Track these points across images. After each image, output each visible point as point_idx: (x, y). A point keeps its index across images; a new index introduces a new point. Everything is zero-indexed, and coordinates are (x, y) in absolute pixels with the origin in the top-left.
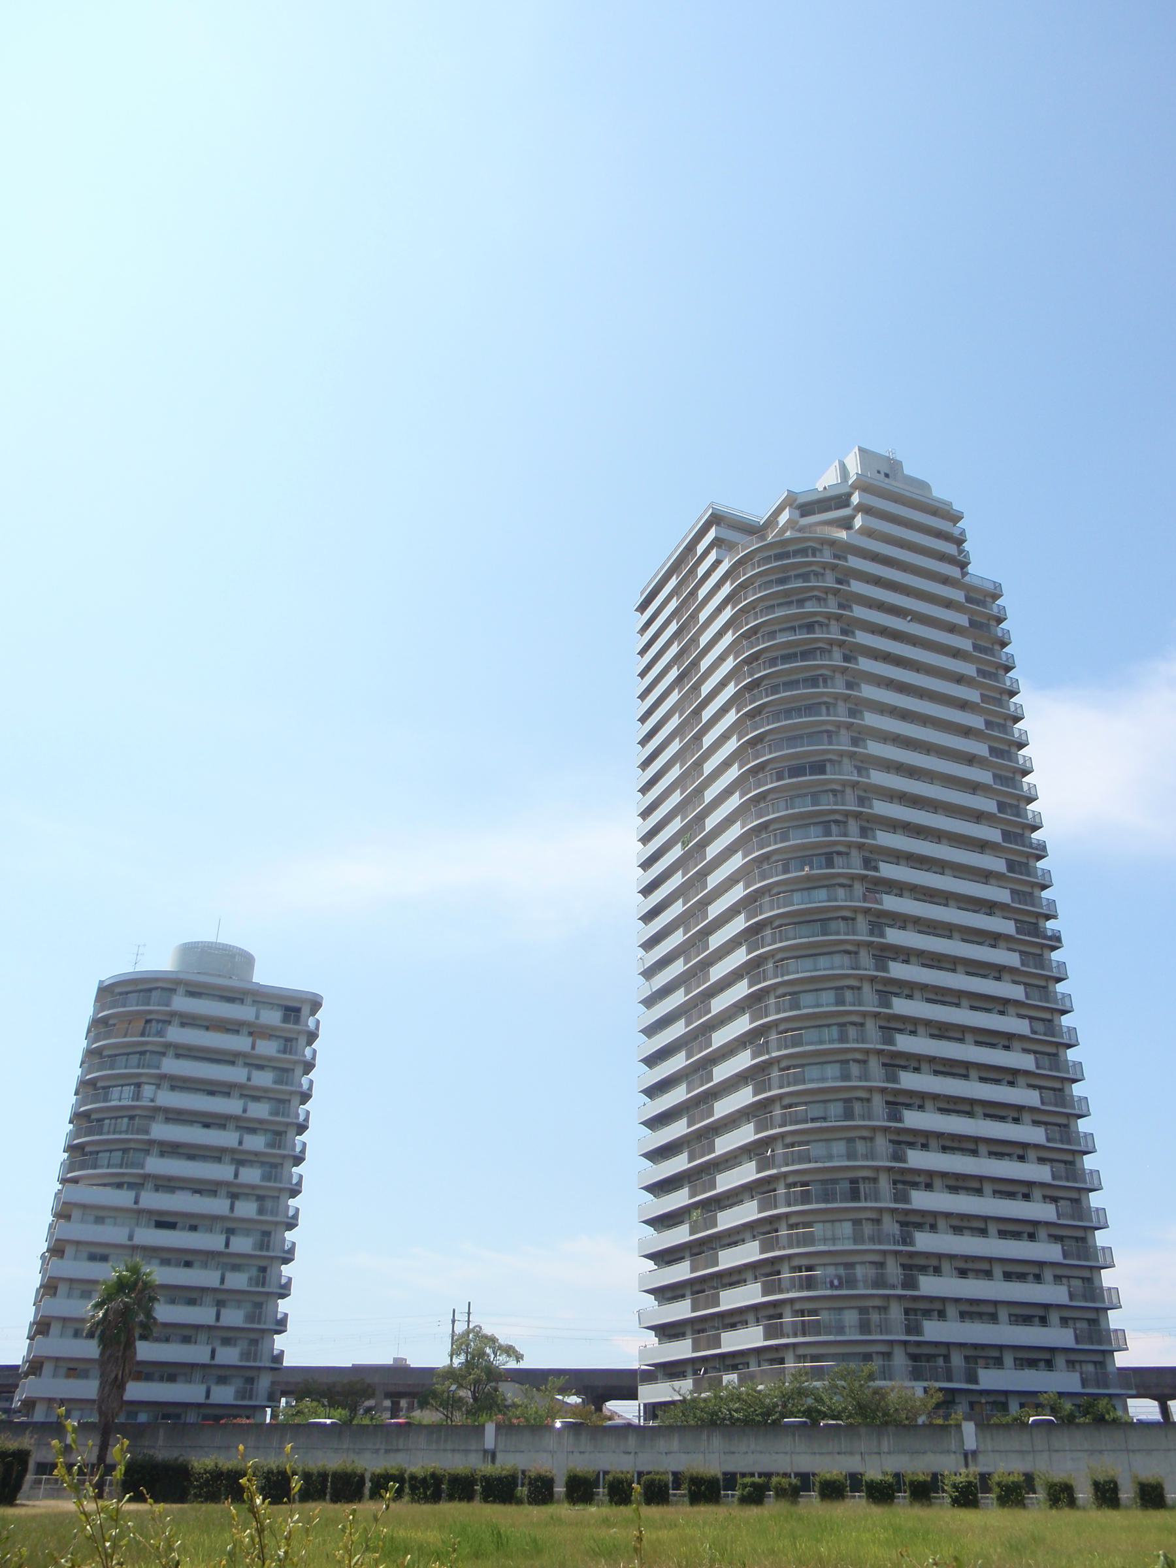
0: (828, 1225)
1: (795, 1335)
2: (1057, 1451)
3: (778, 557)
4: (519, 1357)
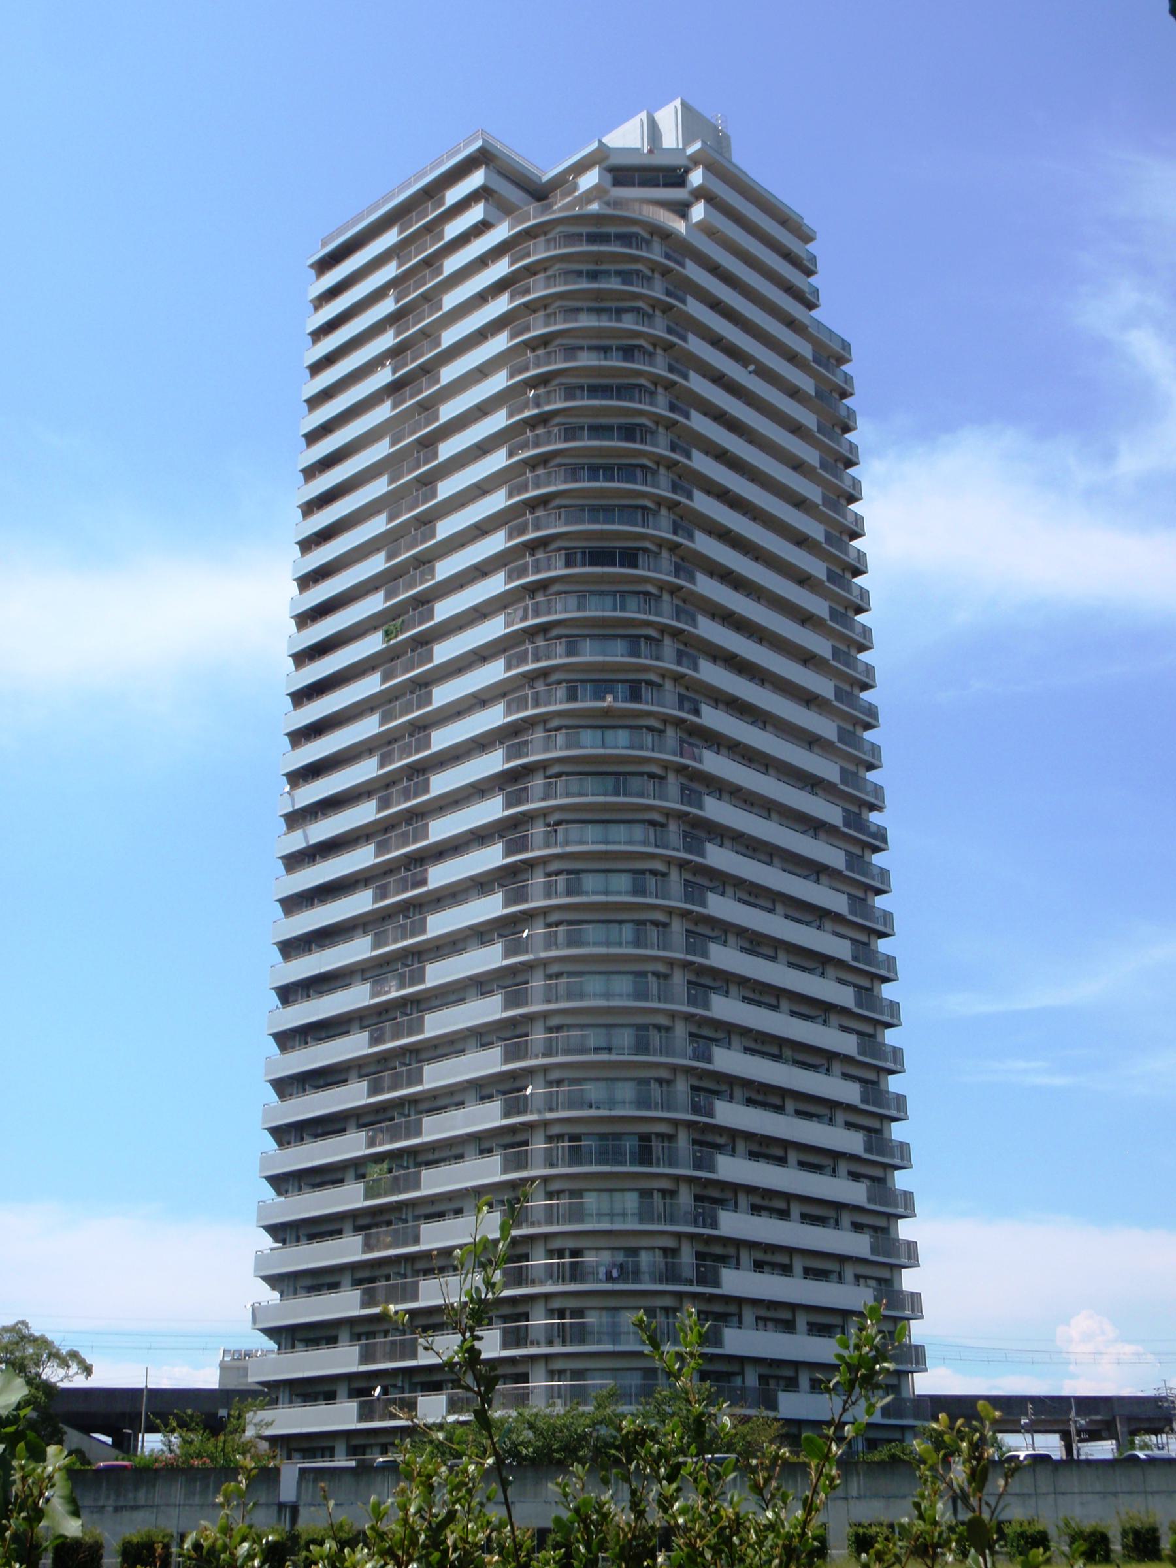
0: (605, 1196)
1: (550, 1343)
2: (1063, 1494)
3: (593, 238)
4: (88, 1370)
